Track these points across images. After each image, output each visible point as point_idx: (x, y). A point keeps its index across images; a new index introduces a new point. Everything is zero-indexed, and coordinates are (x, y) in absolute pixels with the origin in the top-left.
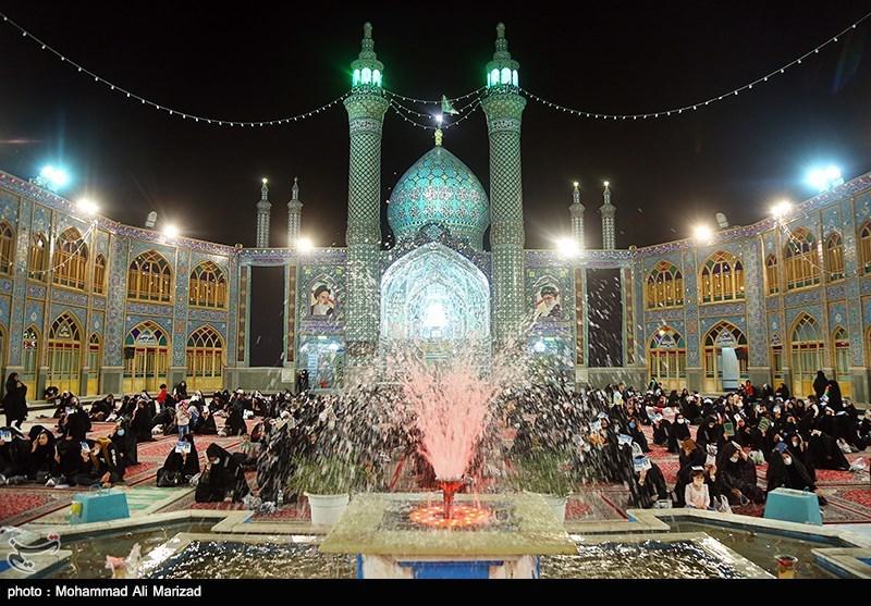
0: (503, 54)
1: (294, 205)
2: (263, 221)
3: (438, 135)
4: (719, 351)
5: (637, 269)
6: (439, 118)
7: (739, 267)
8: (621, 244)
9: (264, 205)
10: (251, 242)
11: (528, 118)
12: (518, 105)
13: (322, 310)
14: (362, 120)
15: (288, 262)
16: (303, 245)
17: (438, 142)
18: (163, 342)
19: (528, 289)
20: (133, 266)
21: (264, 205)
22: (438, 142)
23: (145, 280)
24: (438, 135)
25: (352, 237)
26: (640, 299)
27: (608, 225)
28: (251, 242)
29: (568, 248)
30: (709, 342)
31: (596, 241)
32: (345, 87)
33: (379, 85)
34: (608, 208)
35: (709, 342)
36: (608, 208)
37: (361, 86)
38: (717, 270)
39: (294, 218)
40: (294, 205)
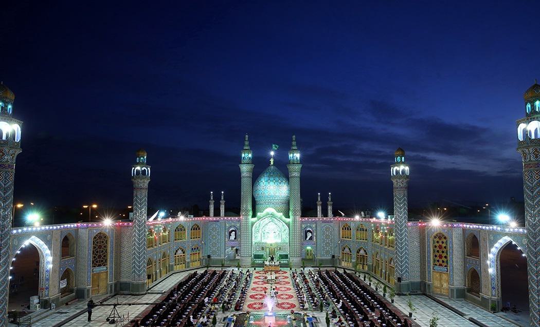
0: (295, 148)
3: (272, 160)
6: (272, 153)
7: (366, 230)
11: (302, 170)
12: (298, 167)
14: (245, 169)
17: (272, 163)
18: (184, 253)
20: (176, 231)
22: (272, 163)
23: (178, 235)
24: (272, 160)
27: (330, 208)
28: (208, 215)
32: (239, 160)
38: (361, 230)
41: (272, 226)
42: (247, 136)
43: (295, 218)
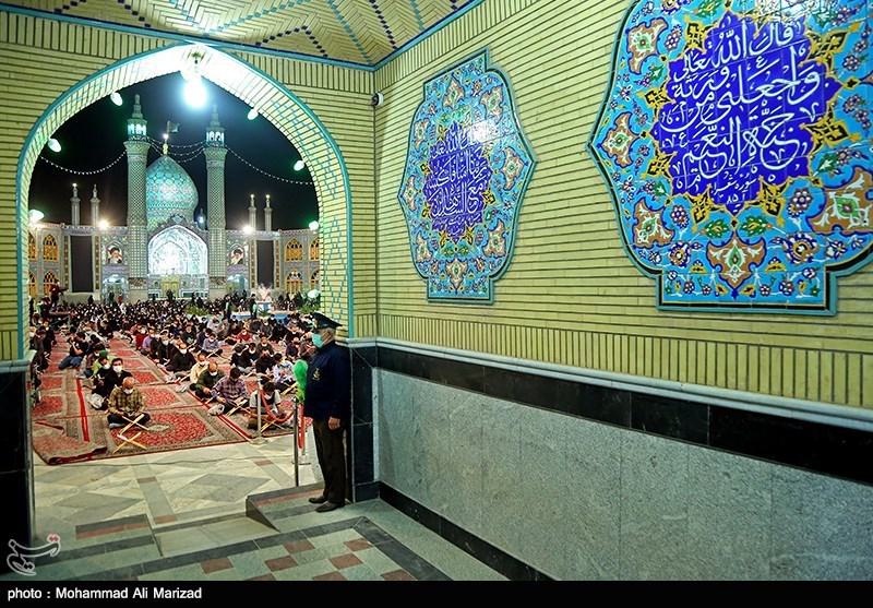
1: (95, 200)
2: (76, 209)
3: (165, 147)
4: (317, 282)
5: (282, 240)
8: (274, 229)
9: (76, 200)
10: (69, 222)
12: (223, 153)
13: (115, 261)
14: (135, 153)
15: (94, 234)
16: (102, 225)
17: (165, 152)
19: (227, 247)
21: (76, 200)
22: (165, 152)
24: (165, 147)
25: (131, 220)
26: (283, 255)
27: (268, 218)
28: (69, 222)
29: (248, 229)
30: (313, 278)
31: (261, 225)
33: (145, 134)
34: (268, 209)
35: (313, 278)
36: (268, 209)
37: (136, 135)
39: (95, 209)
40: (95, 200)
41: (169, 248)
42: (138, 97)
43: (219, 233)
